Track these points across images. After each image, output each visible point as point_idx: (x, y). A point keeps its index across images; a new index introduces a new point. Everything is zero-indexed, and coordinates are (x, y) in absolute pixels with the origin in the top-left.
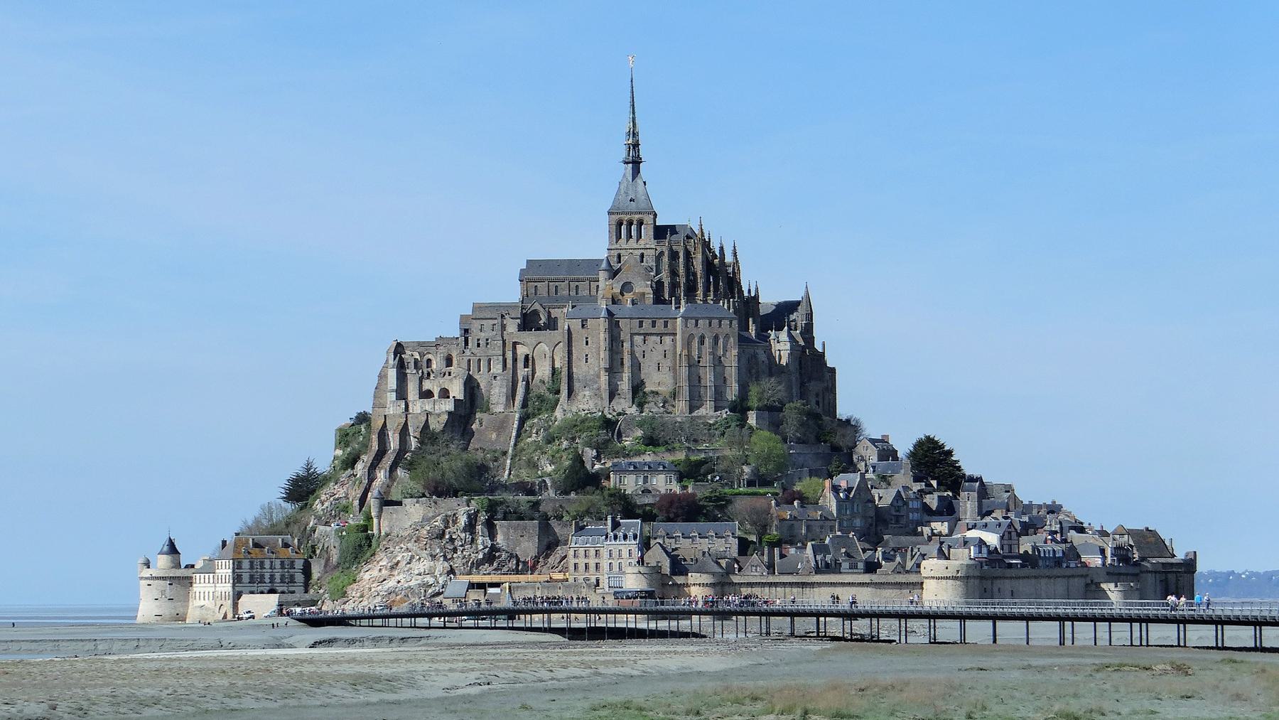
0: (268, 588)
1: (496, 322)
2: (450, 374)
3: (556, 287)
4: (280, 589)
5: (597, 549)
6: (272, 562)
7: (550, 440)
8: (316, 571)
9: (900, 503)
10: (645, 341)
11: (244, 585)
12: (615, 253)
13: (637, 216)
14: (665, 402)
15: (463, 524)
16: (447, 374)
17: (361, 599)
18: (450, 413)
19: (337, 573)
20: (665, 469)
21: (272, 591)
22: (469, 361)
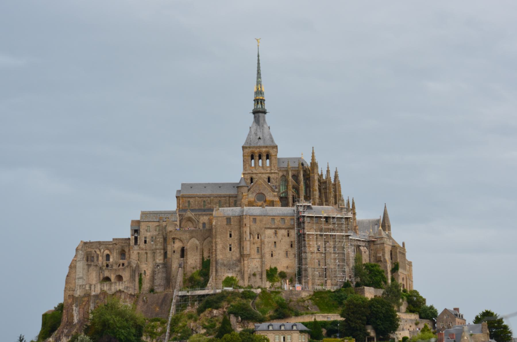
1: (157, 224)
2: (123, 265)
3: (204, 201)
10: (276, 233)
12: (248, 177)
16: (121, 265)
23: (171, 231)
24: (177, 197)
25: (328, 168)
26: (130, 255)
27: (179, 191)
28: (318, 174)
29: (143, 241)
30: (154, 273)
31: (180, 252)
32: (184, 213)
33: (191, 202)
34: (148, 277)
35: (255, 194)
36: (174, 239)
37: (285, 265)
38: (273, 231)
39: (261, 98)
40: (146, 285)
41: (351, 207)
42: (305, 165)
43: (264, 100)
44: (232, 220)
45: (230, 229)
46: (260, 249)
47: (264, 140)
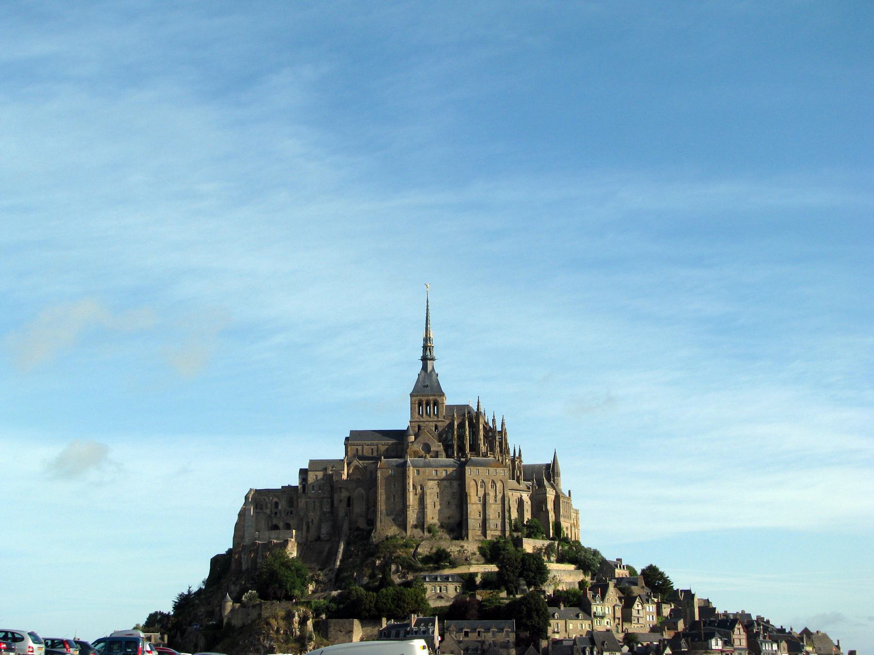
2: (291, 513)
9: (640, 607)
12: (416, 425)
13: (431, 398)
24: (345, 444)
25: (494, 417)
26: (297, 502)
27: (347, 439)
28: (485, 422)
30: (321, 521)
33: (359, 449)
36: (340, 488)
38: (436, 482)
39: (429, 345)
41: (517, 455)
42: (472, 412)
43: (433, 347)
45: (393, 481)
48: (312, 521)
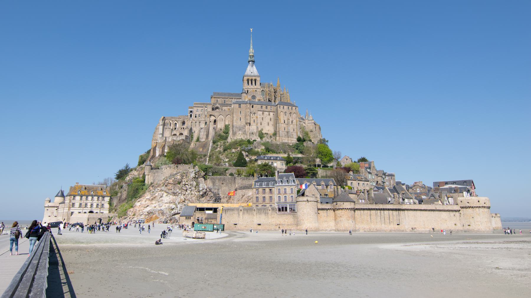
0: (89, 211)
2: (184, 128)
3: (225, 100)
4: (95, 211)
5: (270, 188)
6: (92, 197)
7: (225, 150)
8: (115, 202)
11: (75, 208)
12: (246, 90)
14: (271, 137)
15: (192, 176)
16: (182, 128)
17: (134, 217)
18: (183, 140)
19: (124, 203)
20: (282, 159)
21: (91, 212)
22: (192, 122)
23: (209, 111)
29: (195, 116)
31: (213, 122)
32: (215, 105)
34: (196, 134)
35: (251, 96)
36: (211, 115)
37: (268, 130)
38: (262, 112)
39: (253, 55)
40: (195, 138)
44: (241, 106)
46: (255, 120)
47: (254, 73)
48: (195, 132)
